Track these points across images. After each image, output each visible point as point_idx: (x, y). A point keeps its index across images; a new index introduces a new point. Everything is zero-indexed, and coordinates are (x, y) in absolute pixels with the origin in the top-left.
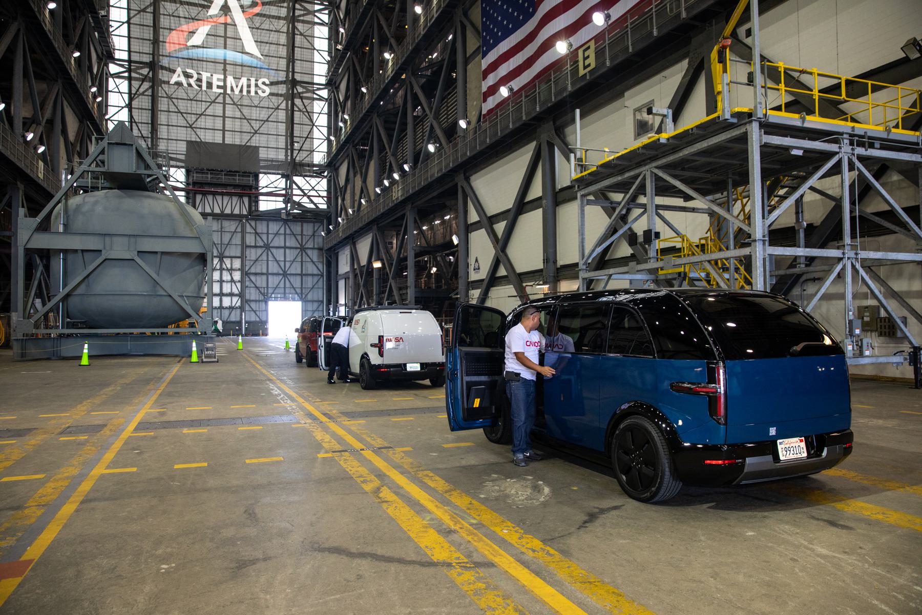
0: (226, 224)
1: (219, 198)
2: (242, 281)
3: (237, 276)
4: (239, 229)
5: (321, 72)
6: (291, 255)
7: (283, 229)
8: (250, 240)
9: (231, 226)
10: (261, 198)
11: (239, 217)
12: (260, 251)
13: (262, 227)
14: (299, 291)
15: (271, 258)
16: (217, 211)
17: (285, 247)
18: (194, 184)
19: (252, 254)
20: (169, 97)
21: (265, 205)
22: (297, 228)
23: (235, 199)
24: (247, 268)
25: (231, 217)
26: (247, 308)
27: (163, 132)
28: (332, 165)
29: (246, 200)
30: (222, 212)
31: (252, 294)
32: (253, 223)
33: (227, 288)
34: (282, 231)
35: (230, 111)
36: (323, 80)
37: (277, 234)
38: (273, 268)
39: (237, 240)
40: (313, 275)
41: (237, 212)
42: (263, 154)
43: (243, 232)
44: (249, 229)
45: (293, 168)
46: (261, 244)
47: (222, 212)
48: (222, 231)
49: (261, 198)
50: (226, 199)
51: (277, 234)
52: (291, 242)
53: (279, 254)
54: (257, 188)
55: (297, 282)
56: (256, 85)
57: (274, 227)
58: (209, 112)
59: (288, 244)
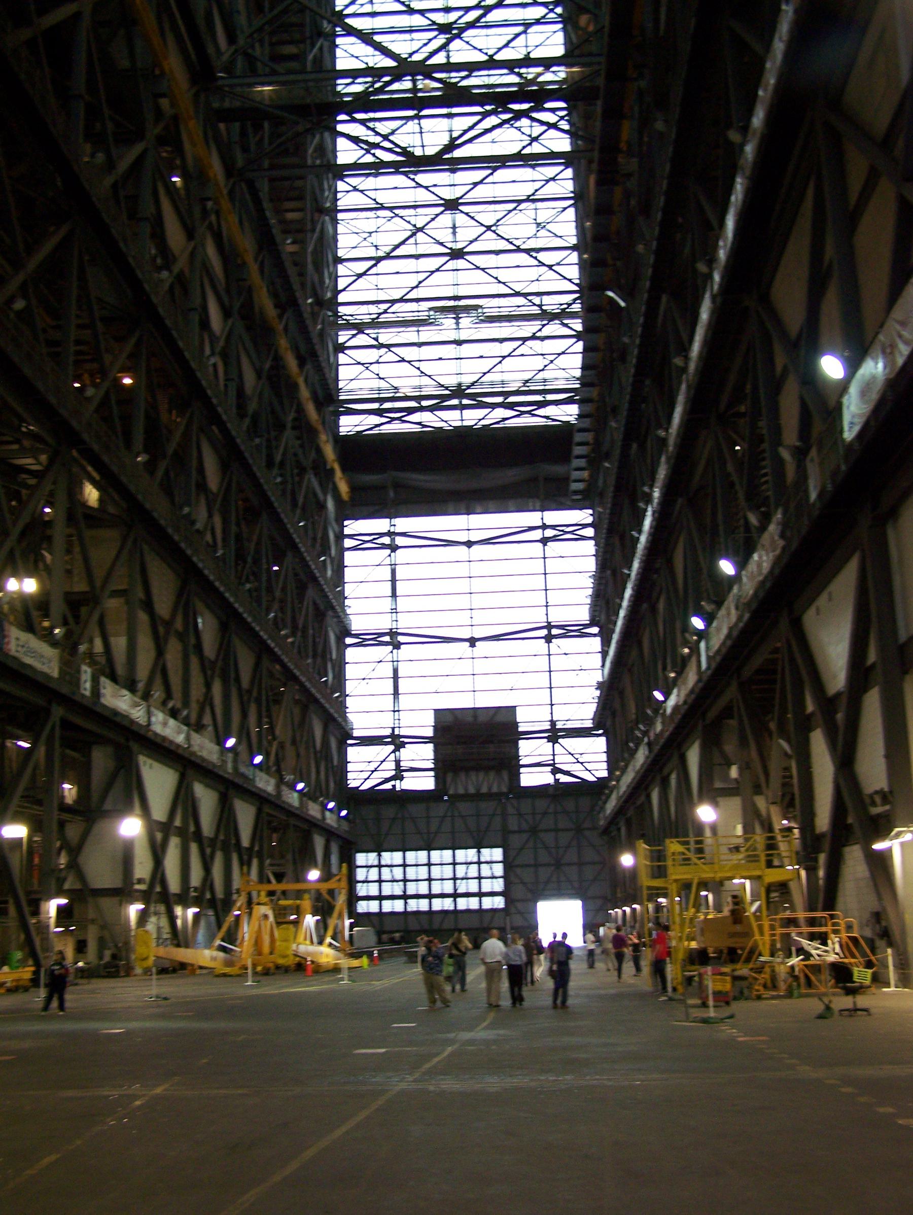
0: (483, 805)
1: (473, 775)
2: (505, 877)
3: (499, 869)
4: (499, 811)
6: (564, 838)
7: (552, 806)
8: (513, 824)
9: (487, 807)
10: (522, 770)
11: (499, 795)
12: (525, 836)
13: (526, 806)
14: (576, 885)
15: (539, 845)
16: (472, 790)
17: (557, 830)
19: (516, 841)
21: (530, 778)
22: (570, 805)
23: (492, 774)
24: (510, 860)
25: (490, 796)
26: (513, 910)
29: (505, 775)
30: (478, 790)
31: (519, 891)
32: (514, 802)
33: (487, 886)
37: (545, 813)
38: (544, 857)
39: (497, 822)
40: (594, 863)
41: (495, 789)
43: (504, 816)
44: (510, 810)
46: (525, 826)
47: (478, 790)
49: (522, 770)
50: (481, 775)
51: (545, 813)
53: (549, 838)
54: (517, 757)
55: (573, 872)
59: (561, 825)
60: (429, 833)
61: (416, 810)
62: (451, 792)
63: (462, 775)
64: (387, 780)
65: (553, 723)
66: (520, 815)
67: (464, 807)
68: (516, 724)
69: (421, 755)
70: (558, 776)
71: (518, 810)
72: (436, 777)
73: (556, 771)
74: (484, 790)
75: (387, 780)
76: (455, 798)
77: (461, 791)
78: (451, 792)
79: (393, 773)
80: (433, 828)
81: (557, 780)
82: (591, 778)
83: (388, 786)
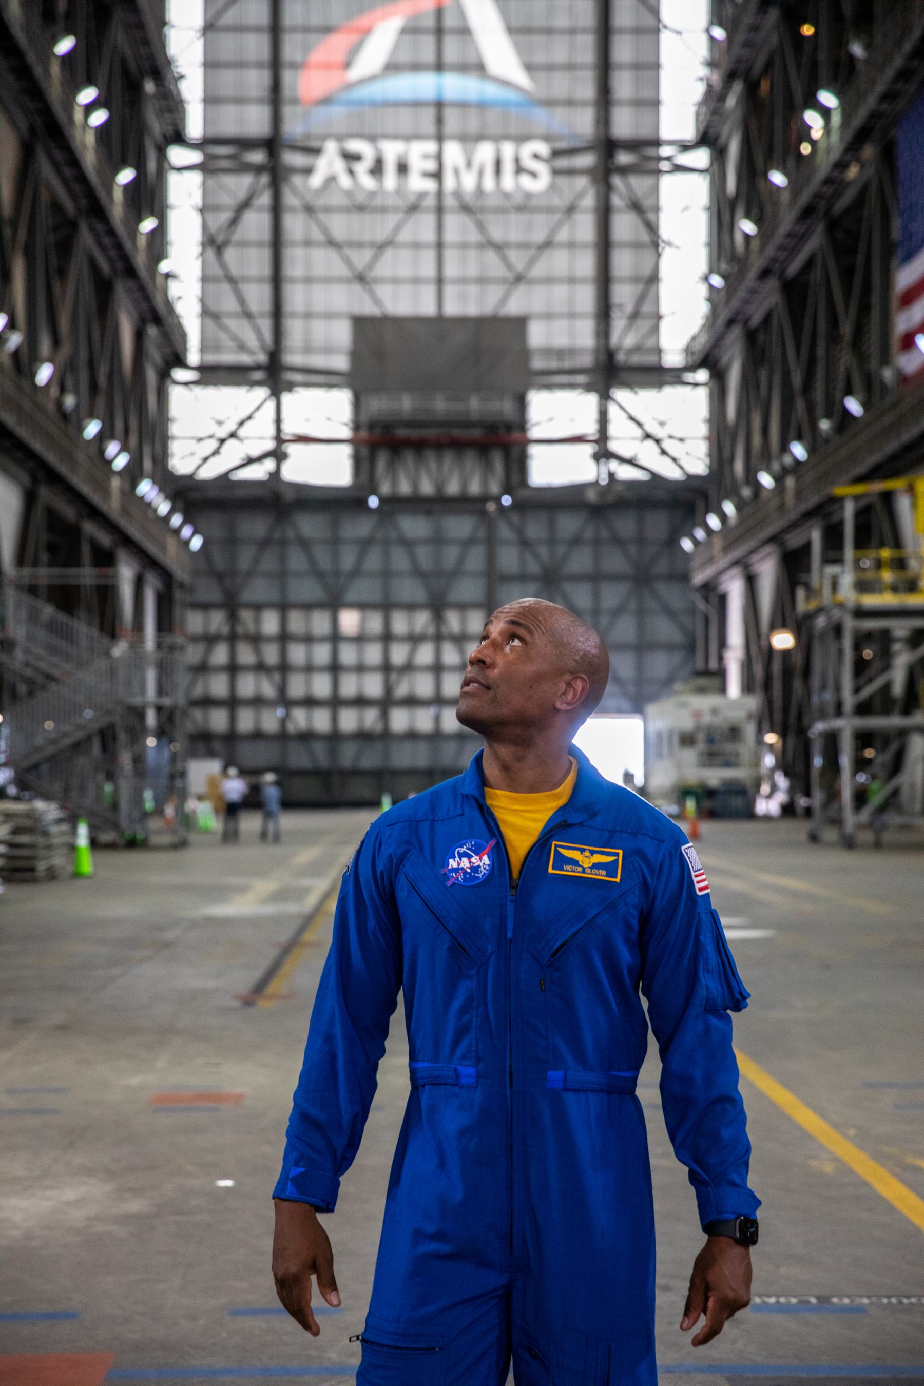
4: (481, 534)
5: (678, 117)
6: (612, 595)
9: (460, 526)
13: (535, 529)
16: (427, 488)
18: (372, 426)
20: (309, 209)
22: (626, 525)
27: (296, 297)
28: (708, 359)
34: (589, 533)
35: (456, 227)
36: (689, 133)
39: (476, 560)
41: (475, 488)
42: (537, 335)
43: (491, 543)
44: (505, 532)
45: (609, 372)
47: (440, 487)
48: (438, 541)
51: (576, 542)
52: (615, 562)
56: (517, 160)
57: (568, 524)
58: (405, 236)
60: (337, 573)
61: (309, 525)
62: (385, 488)
63: (409, 457)
64: (250, 461)
65: (610, 354)
66: (525, 543)
67: (414, 526)
68: (525, 353)
69: (323, 412)
70: (614, 465)
71: (520, 532)
72: (357, 460)
73: (603, 454)
74: (453, 488)
75: (250, 461)
76: (394, 505)
77: (405, 488)
78: (385, 488)
79: (270, 445)
80: (348, 560)
81: (611, 475)
82: (672, 473)
83: (259, 472)
